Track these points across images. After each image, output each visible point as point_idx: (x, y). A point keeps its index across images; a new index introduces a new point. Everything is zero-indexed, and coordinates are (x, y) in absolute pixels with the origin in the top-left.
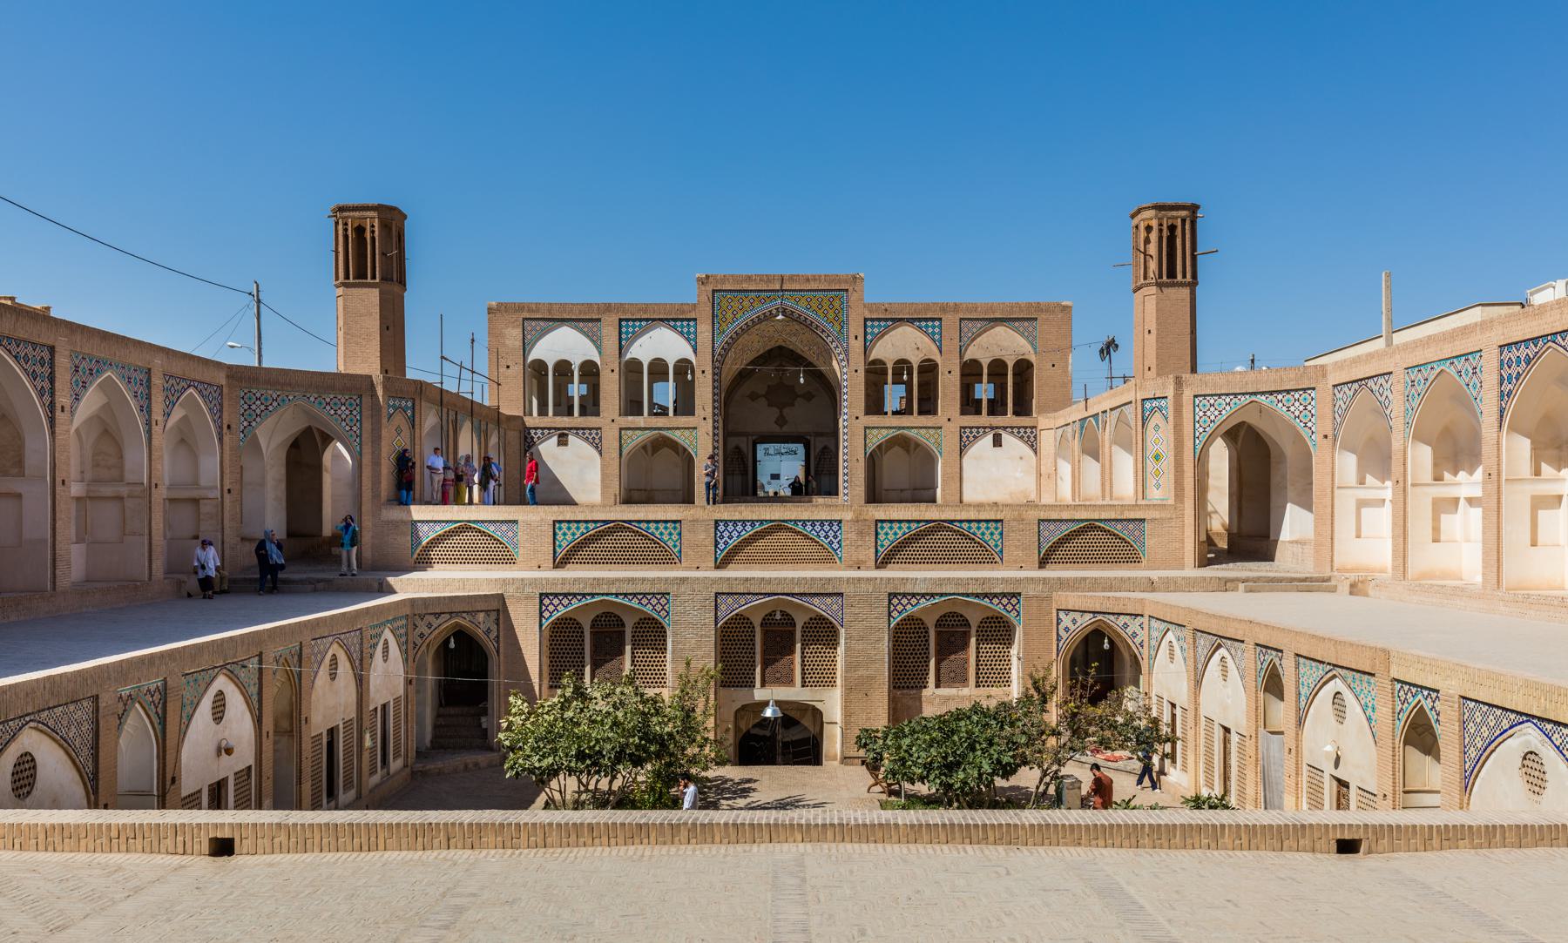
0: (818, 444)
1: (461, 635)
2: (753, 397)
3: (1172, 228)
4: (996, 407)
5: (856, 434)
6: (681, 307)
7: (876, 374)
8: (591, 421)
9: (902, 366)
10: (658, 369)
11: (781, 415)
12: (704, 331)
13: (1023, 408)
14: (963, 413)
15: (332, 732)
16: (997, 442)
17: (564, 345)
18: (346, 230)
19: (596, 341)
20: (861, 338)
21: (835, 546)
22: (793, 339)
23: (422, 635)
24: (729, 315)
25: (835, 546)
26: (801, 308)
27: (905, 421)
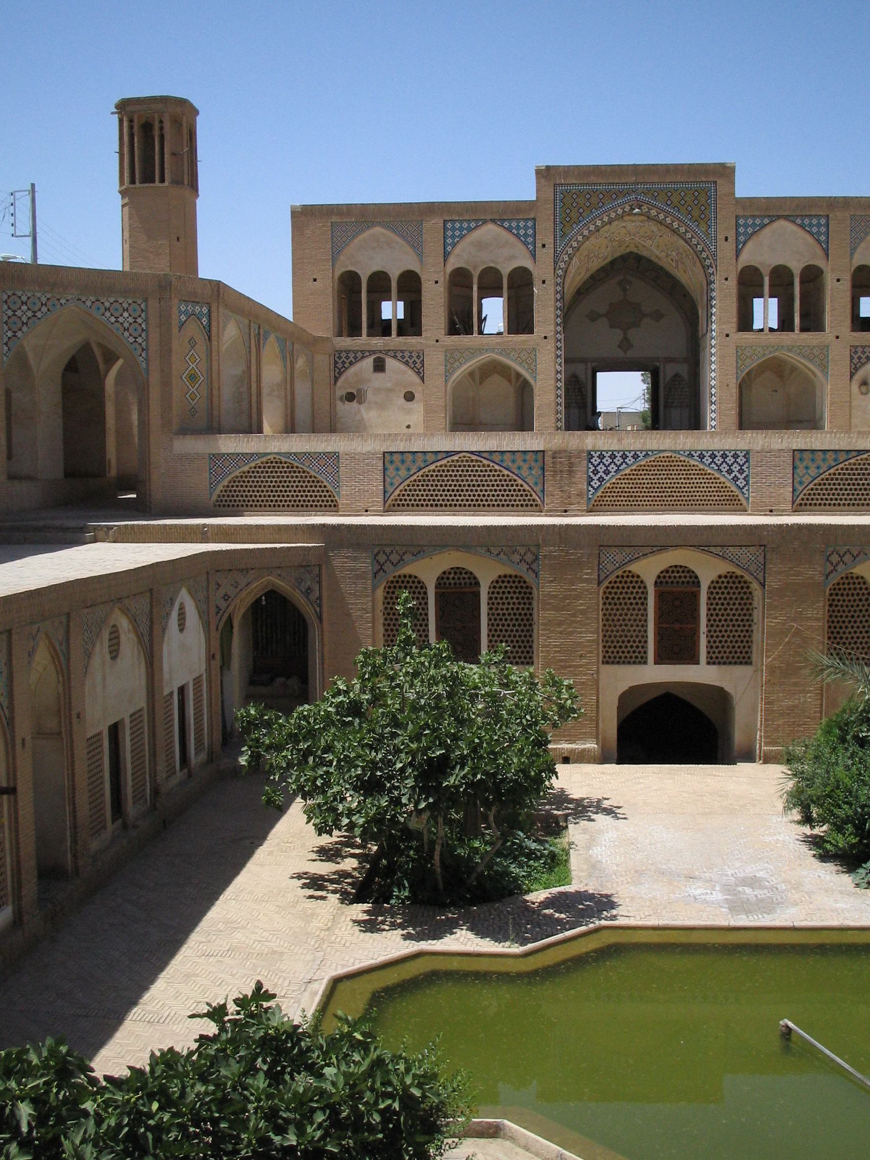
0: (668, 372)
1: (273, 595)
2: (593, 317)
8: (411, 341)
11: (625, 338)
12: (545, 234)
15: (115, 730)
18: (131, 128)
19: (417, 246)
20: (732, 239)
21: (741, 482)
22: (649, 242)
23: (226, 597)
24: (574, 215)
25: (741, 482)
27: (786, 338)
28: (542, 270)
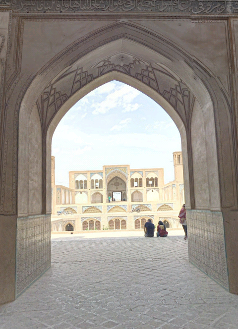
0: (123, 192)
1: (70, 224)
2: (112, 184)
3: (179, 156)
4: (152, 185)
5: (130, 191)
6: (100, 171)
7: (132, 180)
8: (85, 190)
9: (136, 180)
10: (97, 181)
12: (104, 174)
13: (156, 185)
14: (147, 186)
16: (152, 191)
17: (81, 178)
26: (119, 170)
28: (104, 180)
